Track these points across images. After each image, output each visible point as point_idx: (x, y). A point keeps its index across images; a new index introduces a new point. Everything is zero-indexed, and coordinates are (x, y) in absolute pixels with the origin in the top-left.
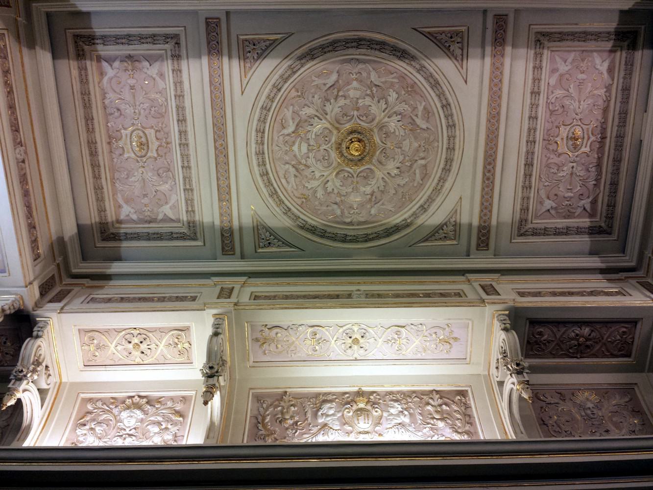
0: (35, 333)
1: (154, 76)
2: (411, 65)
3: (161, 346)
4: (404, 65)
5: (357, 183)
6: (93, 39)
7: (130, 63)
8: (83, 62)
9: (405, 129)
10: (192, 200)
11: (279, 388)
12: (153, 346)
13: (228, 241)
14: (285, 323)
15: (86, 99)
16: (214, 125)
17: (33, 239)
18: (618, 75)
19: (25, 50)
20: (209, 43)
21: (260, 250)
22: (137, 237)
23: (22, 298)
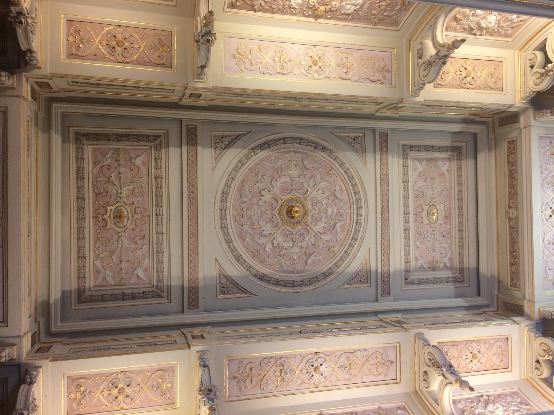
0: (535, 94)
1: (420, 258)
2: (257, 271)
3: (453, 72)
5: (292, 185)
9: (259, 224)
10: (404, 175)
12: (458, 73)
13: (383, 144)
14: (372, 86)
17: (512, 155)
18: (90, 268)
19: (496, 275)
20: (389, 281)
21: (361, 134)
22: (440, 149)
23: (535, 119)
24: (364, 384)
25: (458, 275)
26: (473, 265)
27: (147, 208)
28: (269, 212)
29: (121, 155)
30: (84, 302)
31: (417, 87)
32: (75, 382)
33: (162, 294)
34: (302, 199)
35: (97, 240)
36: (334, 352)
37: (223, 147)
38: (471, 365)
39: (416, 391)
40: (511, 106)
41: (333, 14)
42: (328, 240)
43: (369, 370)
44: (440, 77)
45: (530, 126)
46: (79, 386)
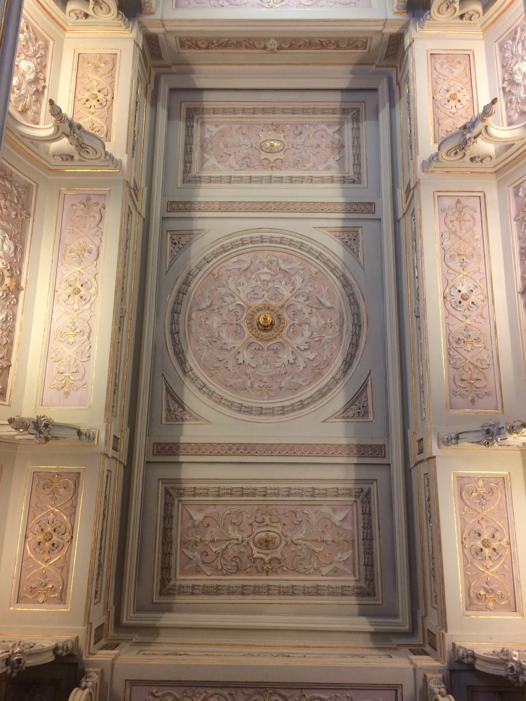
0: (121, 12)
1: (328, 163)
2: (339, 371)
3: (91, 117)
4: (339, 365)
5: (232, 324)
6: (357, 121)
7: (338, 146)
8: (339, 112)
9: (280, 367)
10: (221, 182)
11: (34, 211)
12: (92, 110)
15: (309, 111)
16: (288, 203)
17: (199, 43)
19: (350, 68)
20: (355, 203)
21: (169, 236)
22: (189, 135)
23: (152, 13)
24: (485, 238)
25: (350, 116)
26: (337, 97)
27: (256, 507)
28: (265, 354)
29: (189, 539)
30: (373, 588)
31: (110, 163)
32: (473, 601)
33: (366, 490)
34: (249, 311)
35: (295, 571)
36: (443, 274)
37: (182, 410)
38: (464, 102)
39: (495, 172)
40: (136, 44)
41: (15, 267)
42: (302, 280)
43: (468, 231)
44: (97, 134)
45: (162, 20)
46: (479, 597)
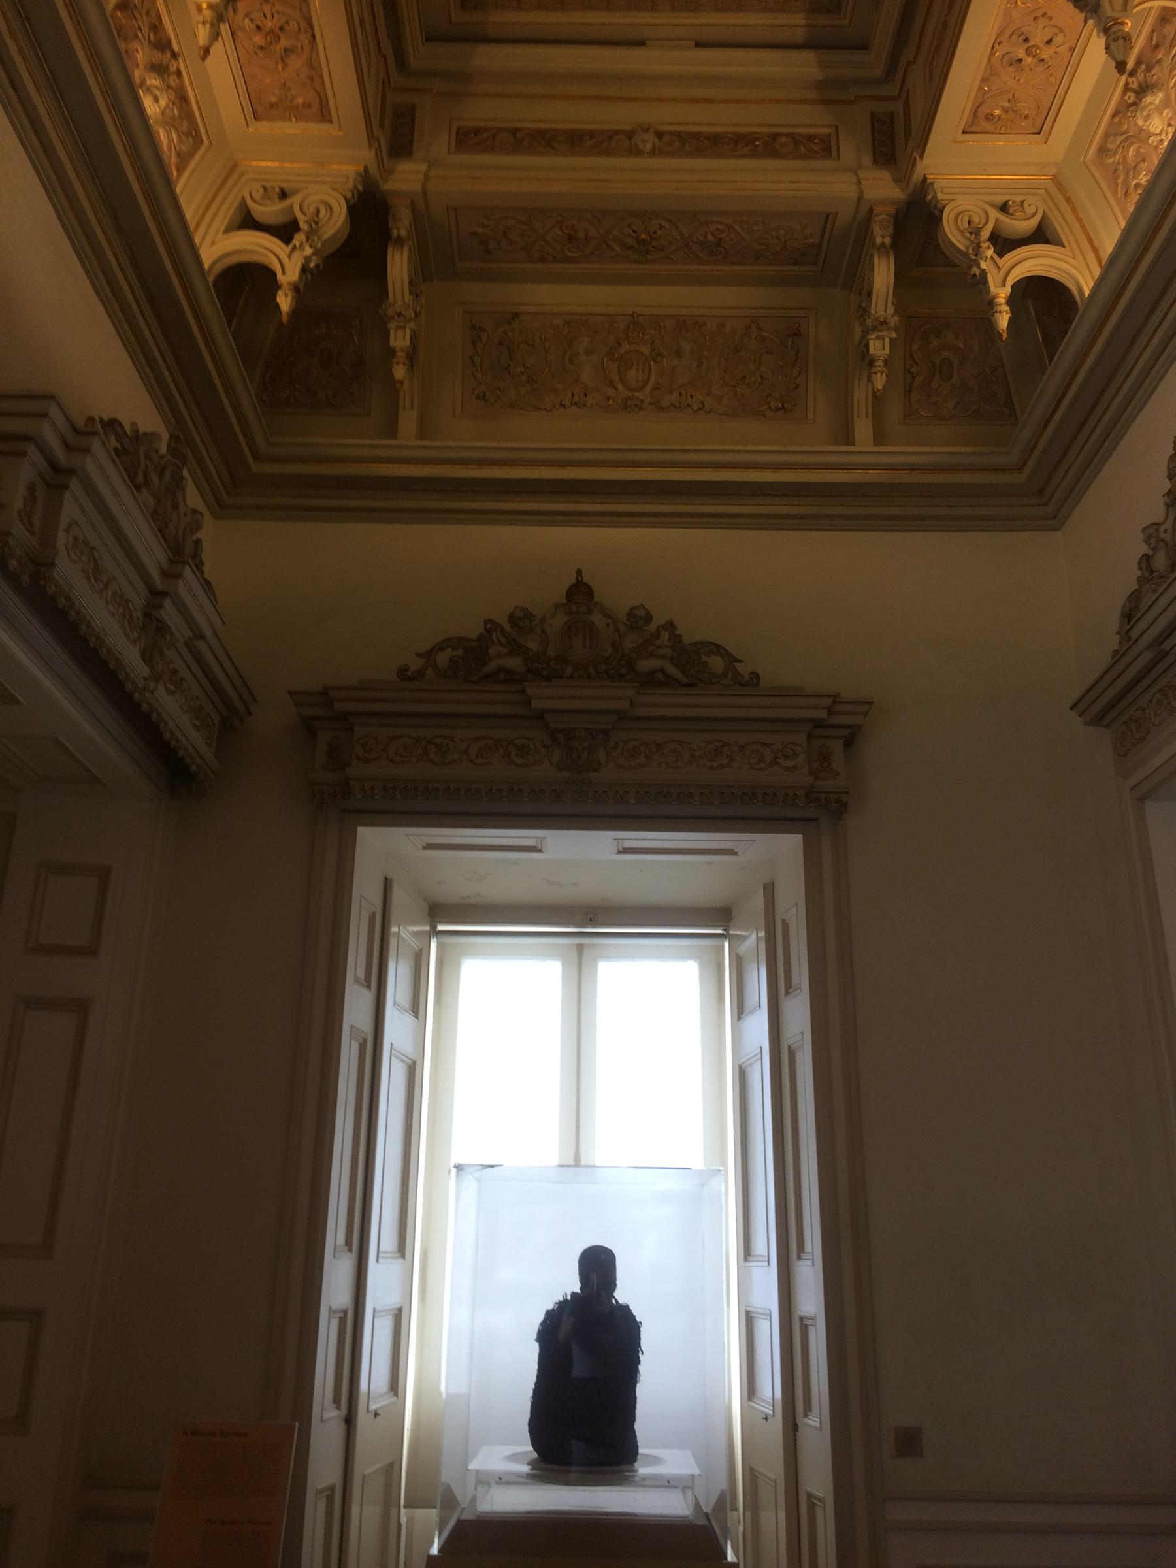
32: (979, 121)
46: (989, 117)
